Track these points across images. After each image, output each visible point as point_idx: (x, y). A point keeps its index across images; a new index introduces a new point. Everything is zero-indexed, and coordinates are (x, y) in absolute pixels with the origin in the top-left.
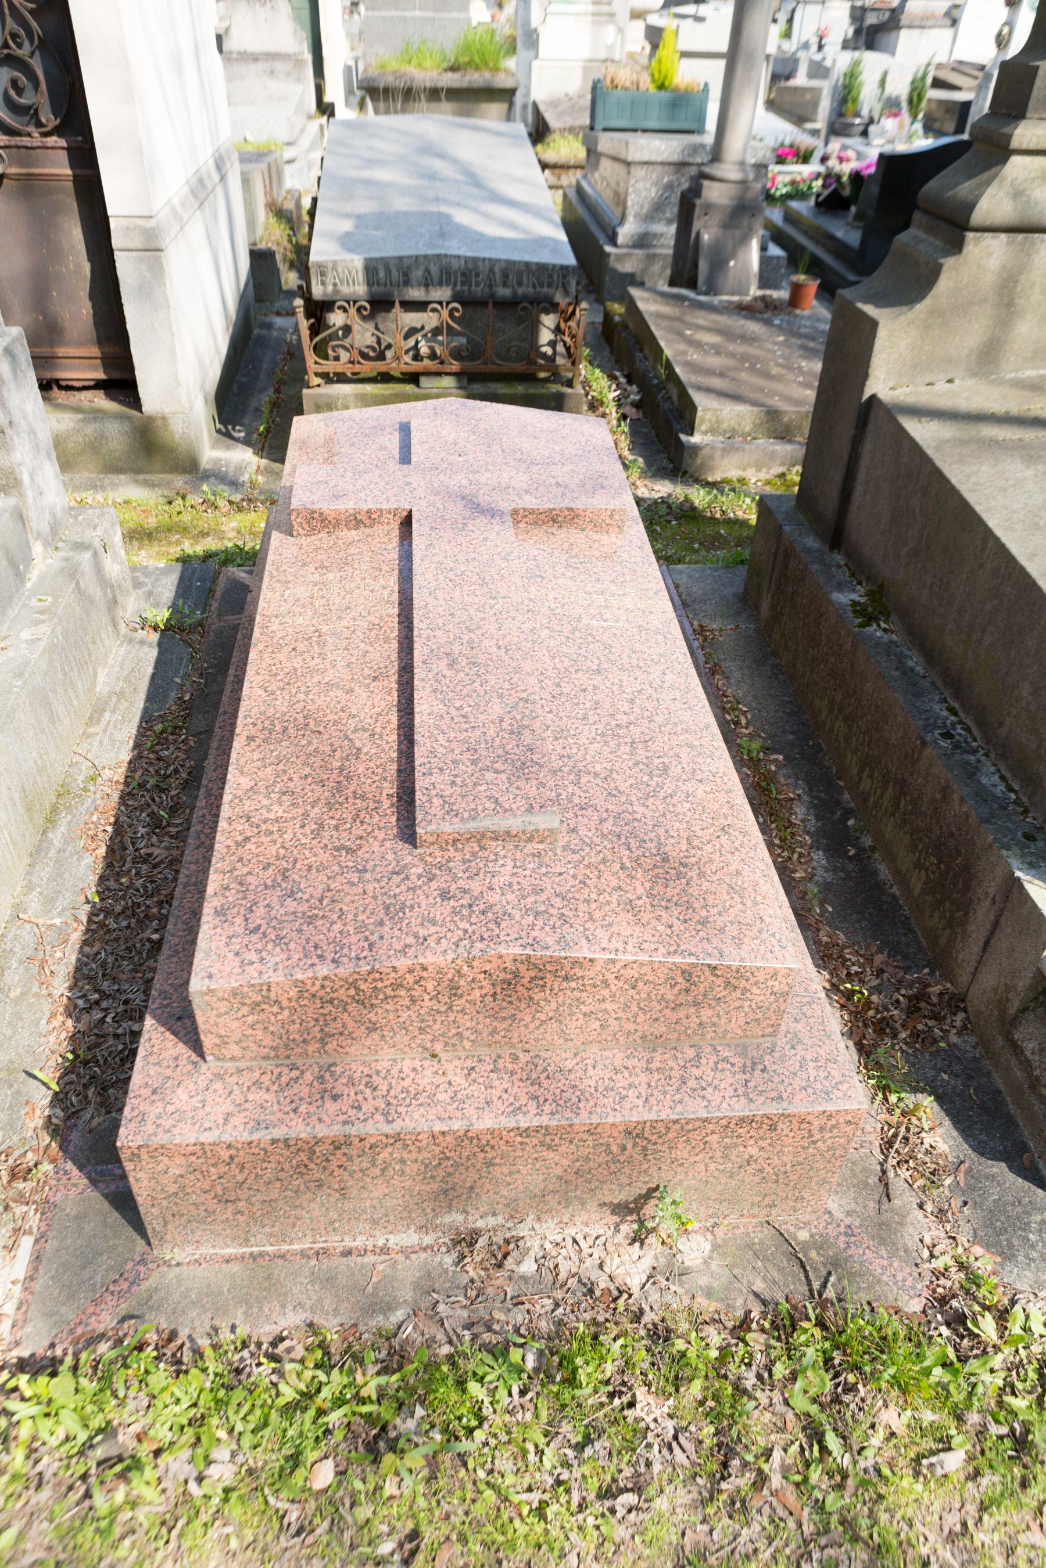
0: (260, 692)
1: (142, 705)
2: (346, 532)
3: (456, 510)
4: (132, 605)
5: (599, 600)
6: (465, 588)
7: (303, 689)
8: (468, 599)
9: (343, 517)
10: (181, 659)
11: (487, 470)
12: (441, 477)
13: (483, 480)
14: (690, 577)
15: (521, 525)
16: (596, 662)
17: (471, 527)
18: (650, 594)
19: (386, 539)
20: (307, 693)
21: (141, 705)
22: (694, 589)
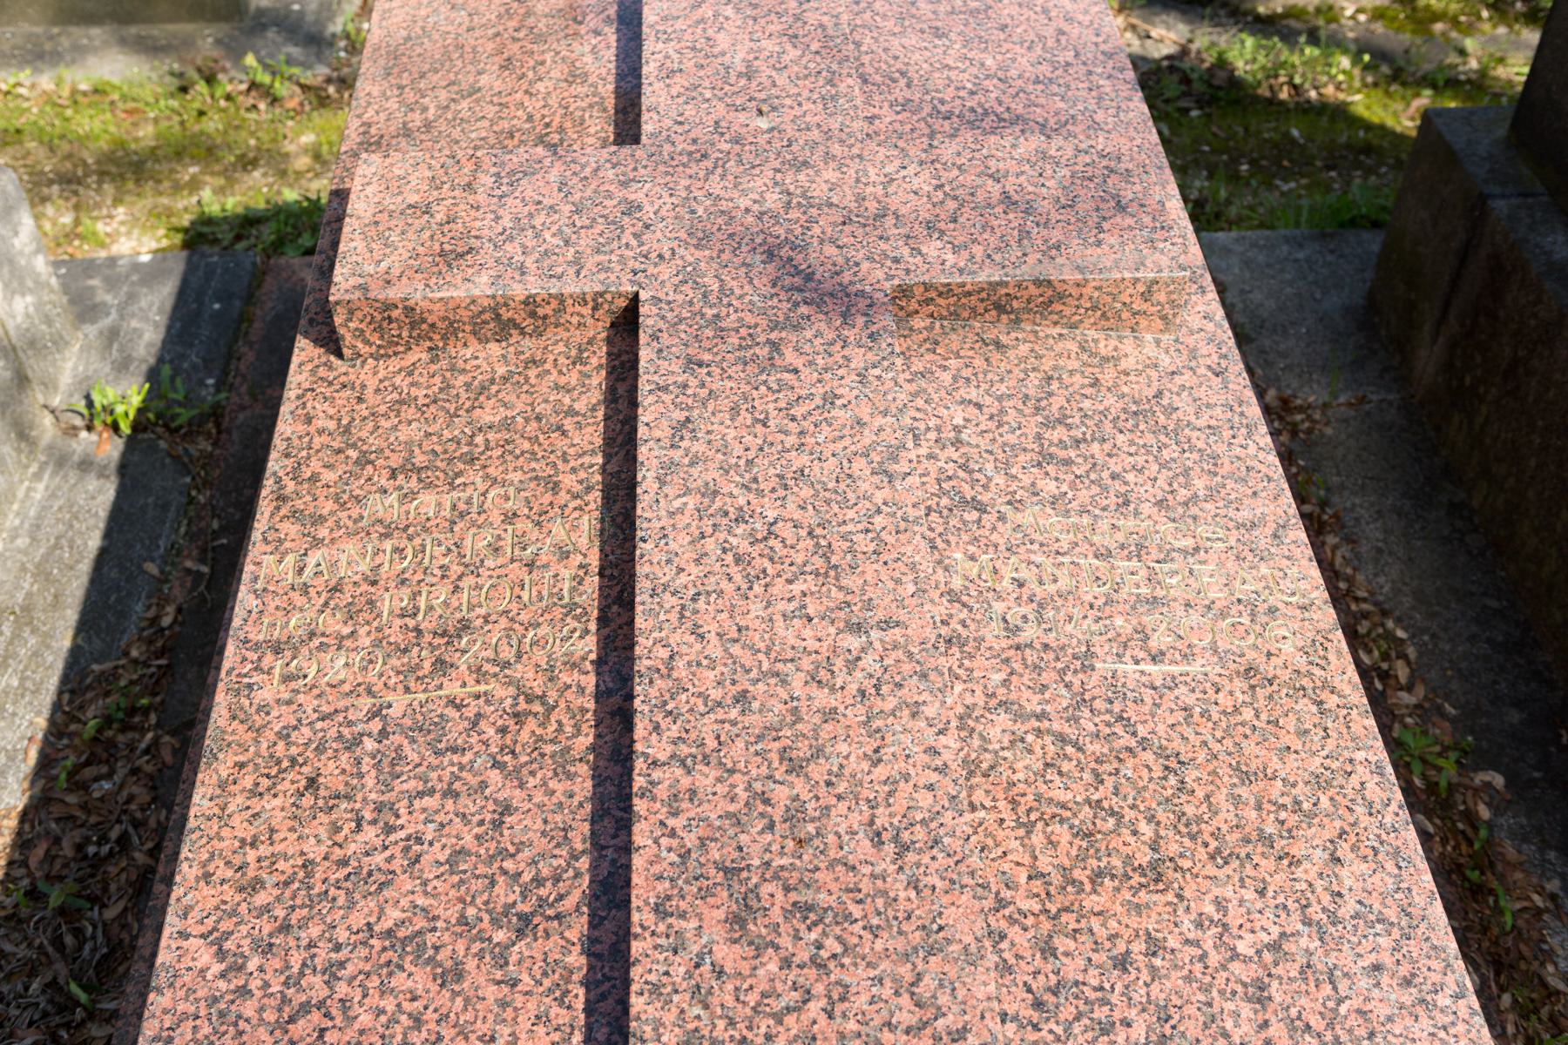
0: (205, 957)
1: (67, 643)
2: (474, 346)
3: (751, 293)
4: (71, 368)
5: (1130, 574)
6: (779, 588)
7: (323, 954)
8: (787, 634)
9: (464, 314)
10: (165, 507)
11: (828, 157)
12: (715, 185)
13: (819, 191)
14: (1247, 263)
15: (918, 323)
16: (1146, 829)
17: (790, 357)
18: (1262, 537)
19: (573, 378)
20: (332, 972)
21: (64, 641)
22: (1257, 296)
